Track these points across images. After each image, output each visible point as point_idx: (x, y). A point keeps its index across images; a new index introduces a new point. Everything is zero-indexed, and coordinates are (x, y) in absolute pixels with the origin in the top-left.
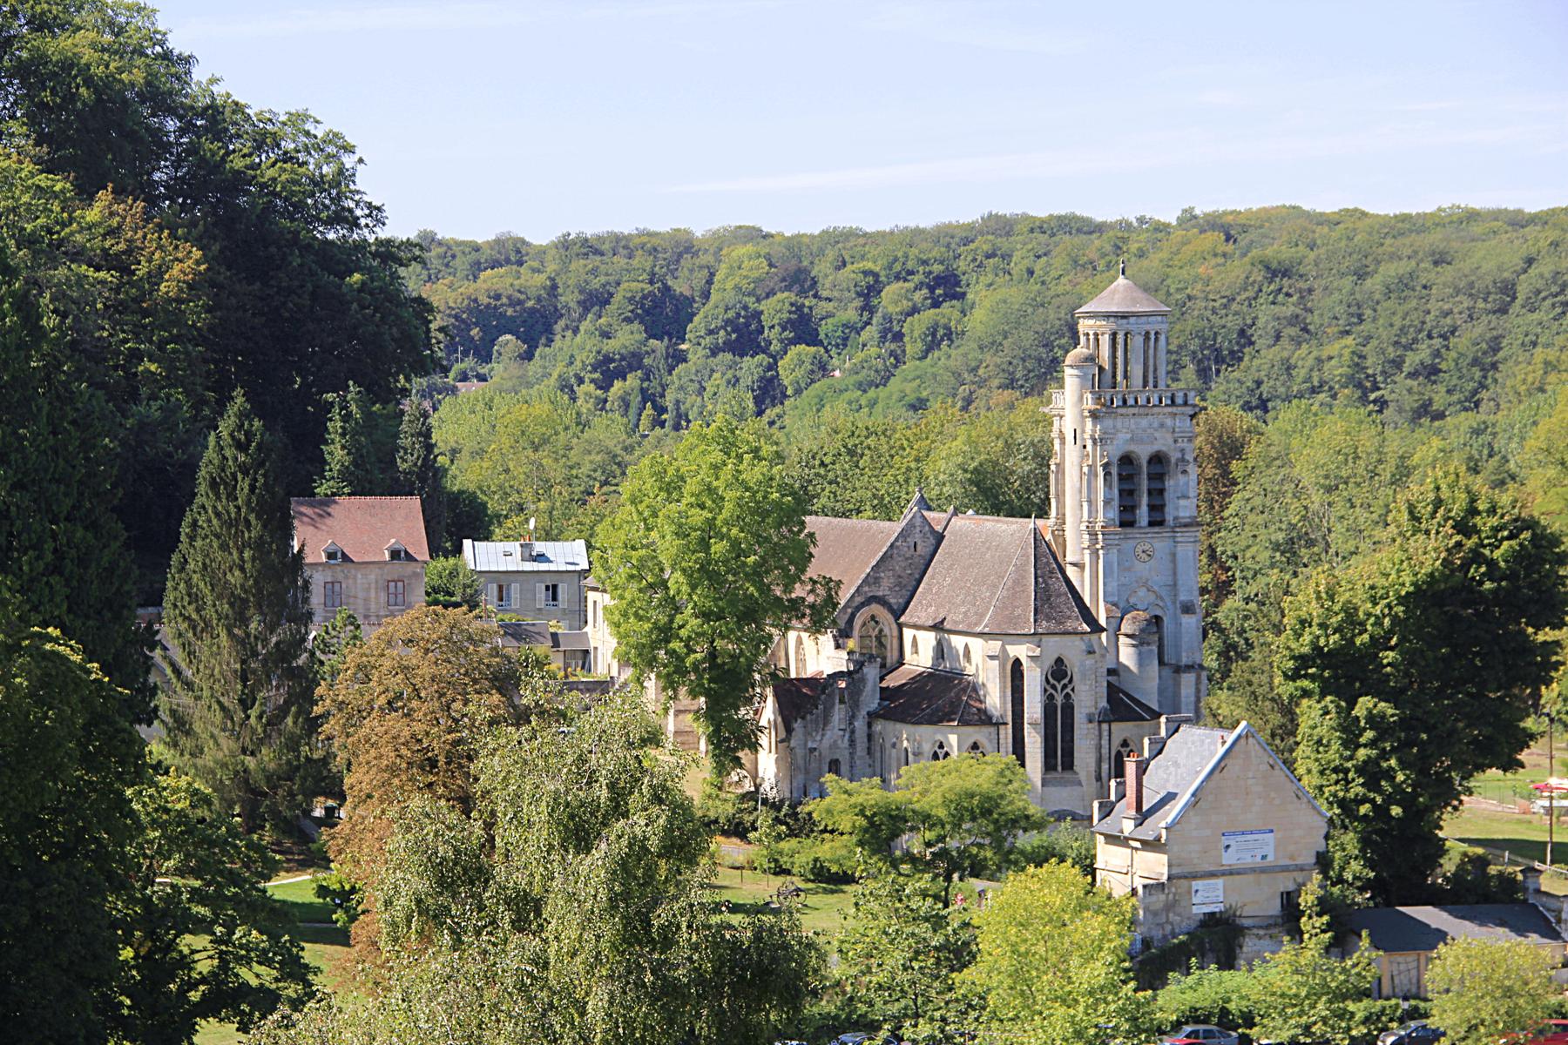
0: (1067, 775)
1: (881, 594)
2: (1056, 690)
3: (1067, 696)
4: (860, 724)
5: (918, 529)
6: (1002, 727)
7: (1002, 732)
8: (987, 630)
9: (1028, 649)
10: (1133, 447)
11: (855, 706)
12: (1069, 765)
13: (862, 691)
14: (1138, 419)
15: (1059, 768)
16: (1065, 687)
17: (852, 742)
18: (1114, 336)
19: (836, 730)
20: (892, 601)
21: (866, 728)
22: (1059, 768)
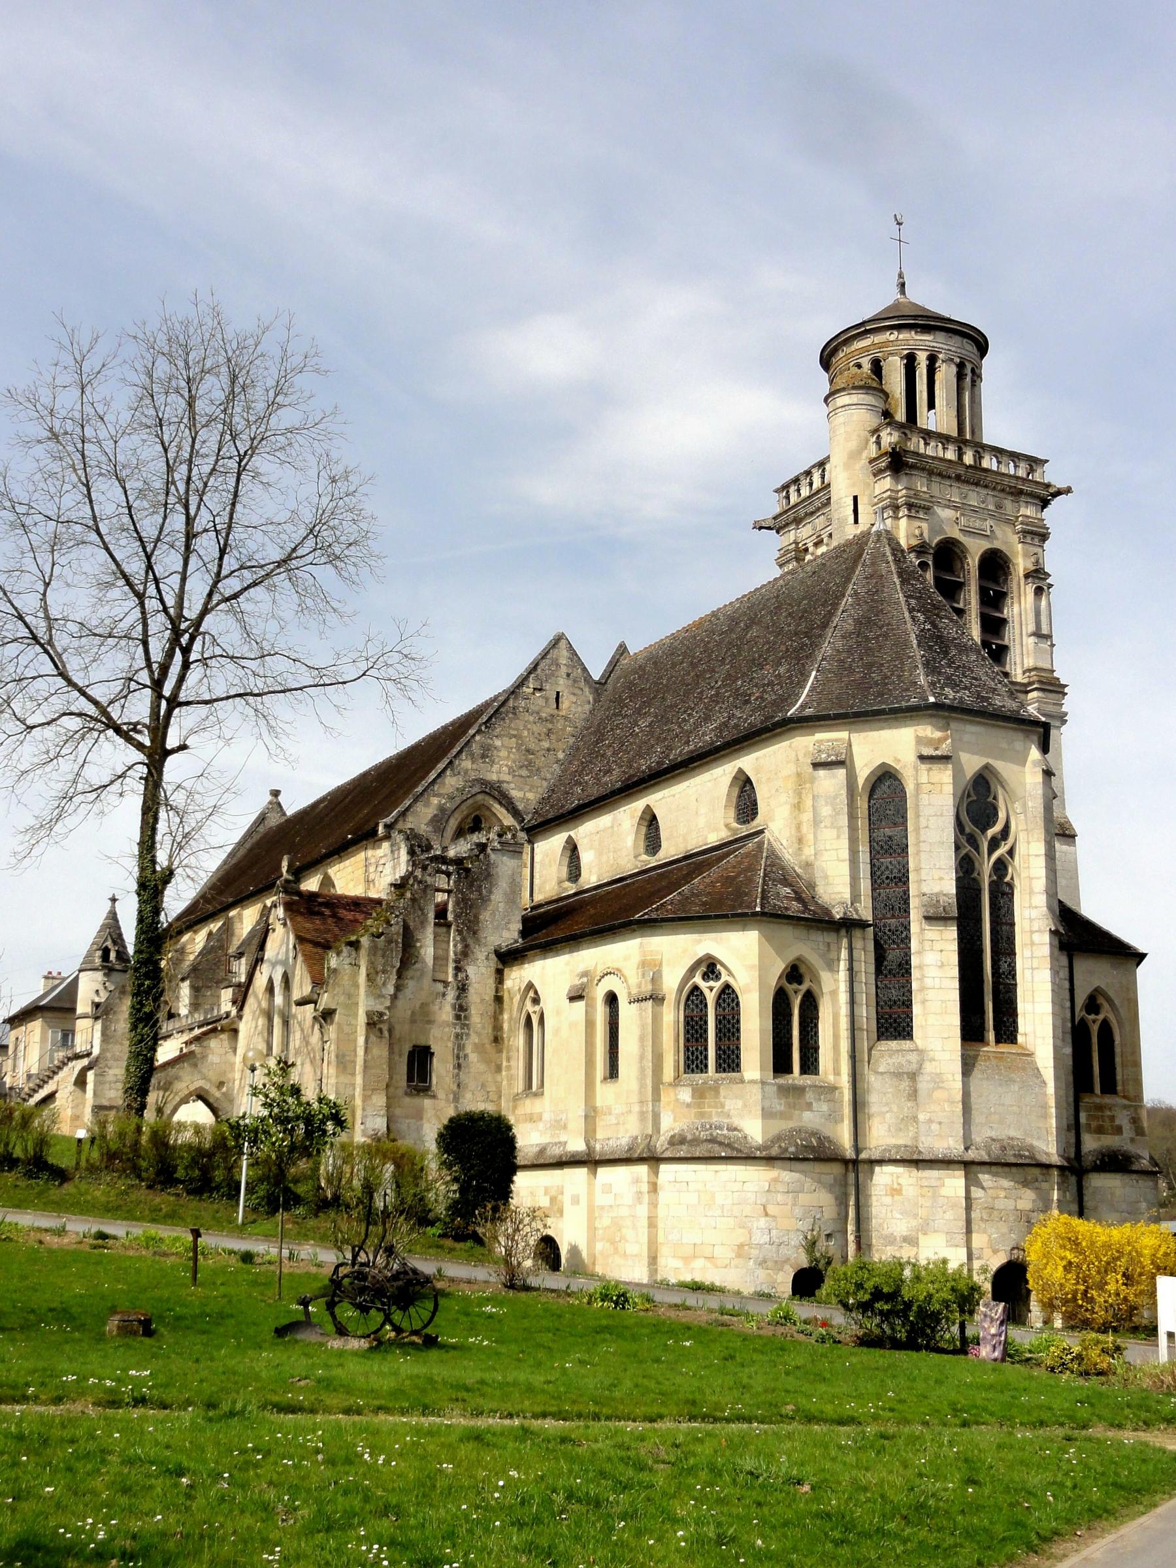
0: (1004, 1048)
1: (494, 777)
2: (977, 848)
3: (1001, 867)
4: (480, 972)
5: (564, 670)
6: (857, 933)
7: (858, 944)
8: (809, 712)
9: (919, 741)
10: (956, 534)
11: (470, 928)
12: (1007, 1031)
13: (485, 900)
14: (965, 488)
15: (991, 1036)
16: (994, 844)
17: (461, 1010)
18: (910, 362)
19: (427, 981)
20: (515, 794)
21: (491, 982)
22: (991, 1036)
